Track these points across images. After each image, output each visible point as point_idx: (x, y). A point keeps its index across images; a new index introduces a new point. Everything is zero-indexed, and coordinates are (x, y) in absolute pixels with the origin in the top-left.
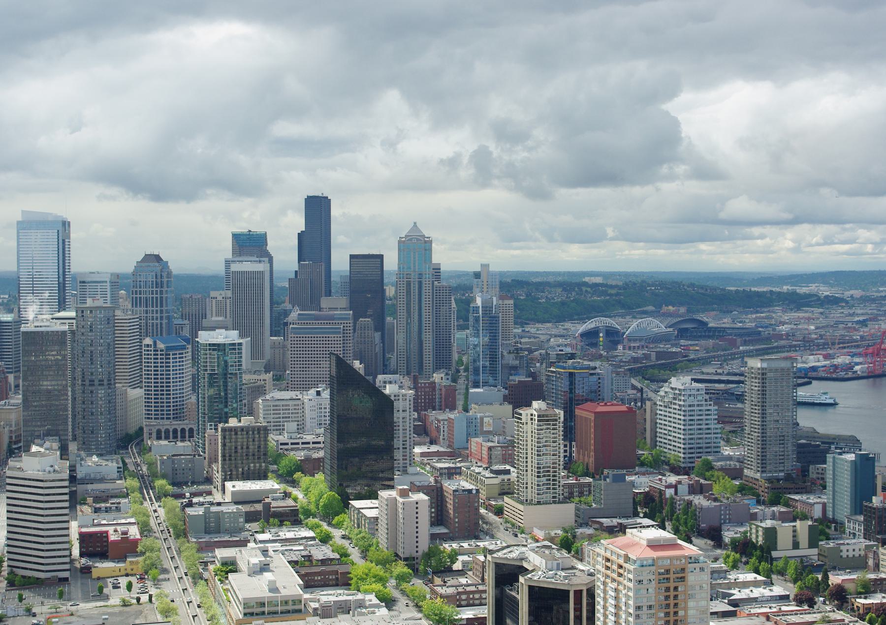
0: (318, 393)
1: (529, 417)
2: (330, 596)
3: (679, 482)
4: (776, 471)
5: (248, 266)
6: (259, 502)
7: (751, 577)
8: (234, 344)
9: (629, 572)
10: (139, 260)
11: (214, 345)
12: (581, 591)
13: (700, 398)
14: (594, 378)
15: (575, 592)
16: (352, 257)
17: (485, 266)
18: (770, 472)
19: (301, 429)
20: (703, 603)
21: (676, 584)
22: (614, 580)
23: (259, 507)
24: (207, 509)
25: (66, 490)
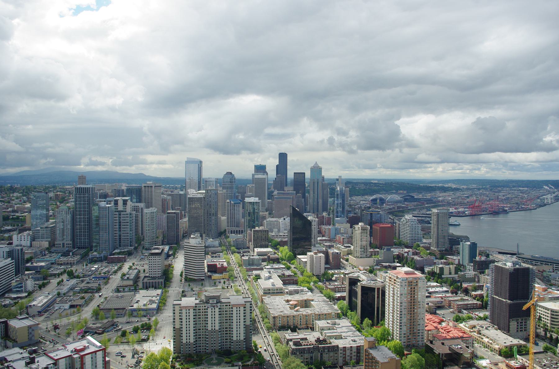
0: (284, 219)
1: (358, 228)
2: (292, 288)
3: (409, 251)
4: (442, 248)
5: (260, 176)
6: (266, 255)
7: (435, 284)
8: (257, 202)
9: (398, 282)
10: (225, 174)
11: (250, 202)
12: (379, 288)
13: (415, 222)
14: (379, 215)
15: (377, 288)
16: (294, 173)
17: (340, 177)
18: (440, 248)
19: (279, 231)
20: (424, 293)
21: (415, 287)
22: (392, 285)
23: (266, 257)
24: (249, 258)
25: (204, 250)
